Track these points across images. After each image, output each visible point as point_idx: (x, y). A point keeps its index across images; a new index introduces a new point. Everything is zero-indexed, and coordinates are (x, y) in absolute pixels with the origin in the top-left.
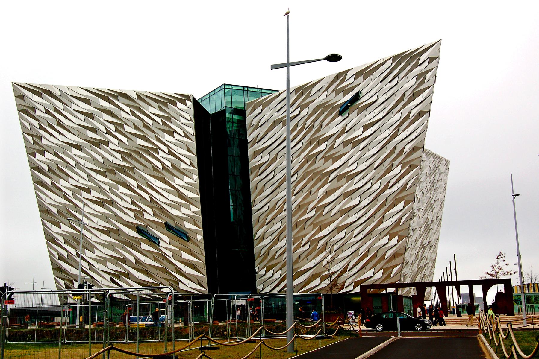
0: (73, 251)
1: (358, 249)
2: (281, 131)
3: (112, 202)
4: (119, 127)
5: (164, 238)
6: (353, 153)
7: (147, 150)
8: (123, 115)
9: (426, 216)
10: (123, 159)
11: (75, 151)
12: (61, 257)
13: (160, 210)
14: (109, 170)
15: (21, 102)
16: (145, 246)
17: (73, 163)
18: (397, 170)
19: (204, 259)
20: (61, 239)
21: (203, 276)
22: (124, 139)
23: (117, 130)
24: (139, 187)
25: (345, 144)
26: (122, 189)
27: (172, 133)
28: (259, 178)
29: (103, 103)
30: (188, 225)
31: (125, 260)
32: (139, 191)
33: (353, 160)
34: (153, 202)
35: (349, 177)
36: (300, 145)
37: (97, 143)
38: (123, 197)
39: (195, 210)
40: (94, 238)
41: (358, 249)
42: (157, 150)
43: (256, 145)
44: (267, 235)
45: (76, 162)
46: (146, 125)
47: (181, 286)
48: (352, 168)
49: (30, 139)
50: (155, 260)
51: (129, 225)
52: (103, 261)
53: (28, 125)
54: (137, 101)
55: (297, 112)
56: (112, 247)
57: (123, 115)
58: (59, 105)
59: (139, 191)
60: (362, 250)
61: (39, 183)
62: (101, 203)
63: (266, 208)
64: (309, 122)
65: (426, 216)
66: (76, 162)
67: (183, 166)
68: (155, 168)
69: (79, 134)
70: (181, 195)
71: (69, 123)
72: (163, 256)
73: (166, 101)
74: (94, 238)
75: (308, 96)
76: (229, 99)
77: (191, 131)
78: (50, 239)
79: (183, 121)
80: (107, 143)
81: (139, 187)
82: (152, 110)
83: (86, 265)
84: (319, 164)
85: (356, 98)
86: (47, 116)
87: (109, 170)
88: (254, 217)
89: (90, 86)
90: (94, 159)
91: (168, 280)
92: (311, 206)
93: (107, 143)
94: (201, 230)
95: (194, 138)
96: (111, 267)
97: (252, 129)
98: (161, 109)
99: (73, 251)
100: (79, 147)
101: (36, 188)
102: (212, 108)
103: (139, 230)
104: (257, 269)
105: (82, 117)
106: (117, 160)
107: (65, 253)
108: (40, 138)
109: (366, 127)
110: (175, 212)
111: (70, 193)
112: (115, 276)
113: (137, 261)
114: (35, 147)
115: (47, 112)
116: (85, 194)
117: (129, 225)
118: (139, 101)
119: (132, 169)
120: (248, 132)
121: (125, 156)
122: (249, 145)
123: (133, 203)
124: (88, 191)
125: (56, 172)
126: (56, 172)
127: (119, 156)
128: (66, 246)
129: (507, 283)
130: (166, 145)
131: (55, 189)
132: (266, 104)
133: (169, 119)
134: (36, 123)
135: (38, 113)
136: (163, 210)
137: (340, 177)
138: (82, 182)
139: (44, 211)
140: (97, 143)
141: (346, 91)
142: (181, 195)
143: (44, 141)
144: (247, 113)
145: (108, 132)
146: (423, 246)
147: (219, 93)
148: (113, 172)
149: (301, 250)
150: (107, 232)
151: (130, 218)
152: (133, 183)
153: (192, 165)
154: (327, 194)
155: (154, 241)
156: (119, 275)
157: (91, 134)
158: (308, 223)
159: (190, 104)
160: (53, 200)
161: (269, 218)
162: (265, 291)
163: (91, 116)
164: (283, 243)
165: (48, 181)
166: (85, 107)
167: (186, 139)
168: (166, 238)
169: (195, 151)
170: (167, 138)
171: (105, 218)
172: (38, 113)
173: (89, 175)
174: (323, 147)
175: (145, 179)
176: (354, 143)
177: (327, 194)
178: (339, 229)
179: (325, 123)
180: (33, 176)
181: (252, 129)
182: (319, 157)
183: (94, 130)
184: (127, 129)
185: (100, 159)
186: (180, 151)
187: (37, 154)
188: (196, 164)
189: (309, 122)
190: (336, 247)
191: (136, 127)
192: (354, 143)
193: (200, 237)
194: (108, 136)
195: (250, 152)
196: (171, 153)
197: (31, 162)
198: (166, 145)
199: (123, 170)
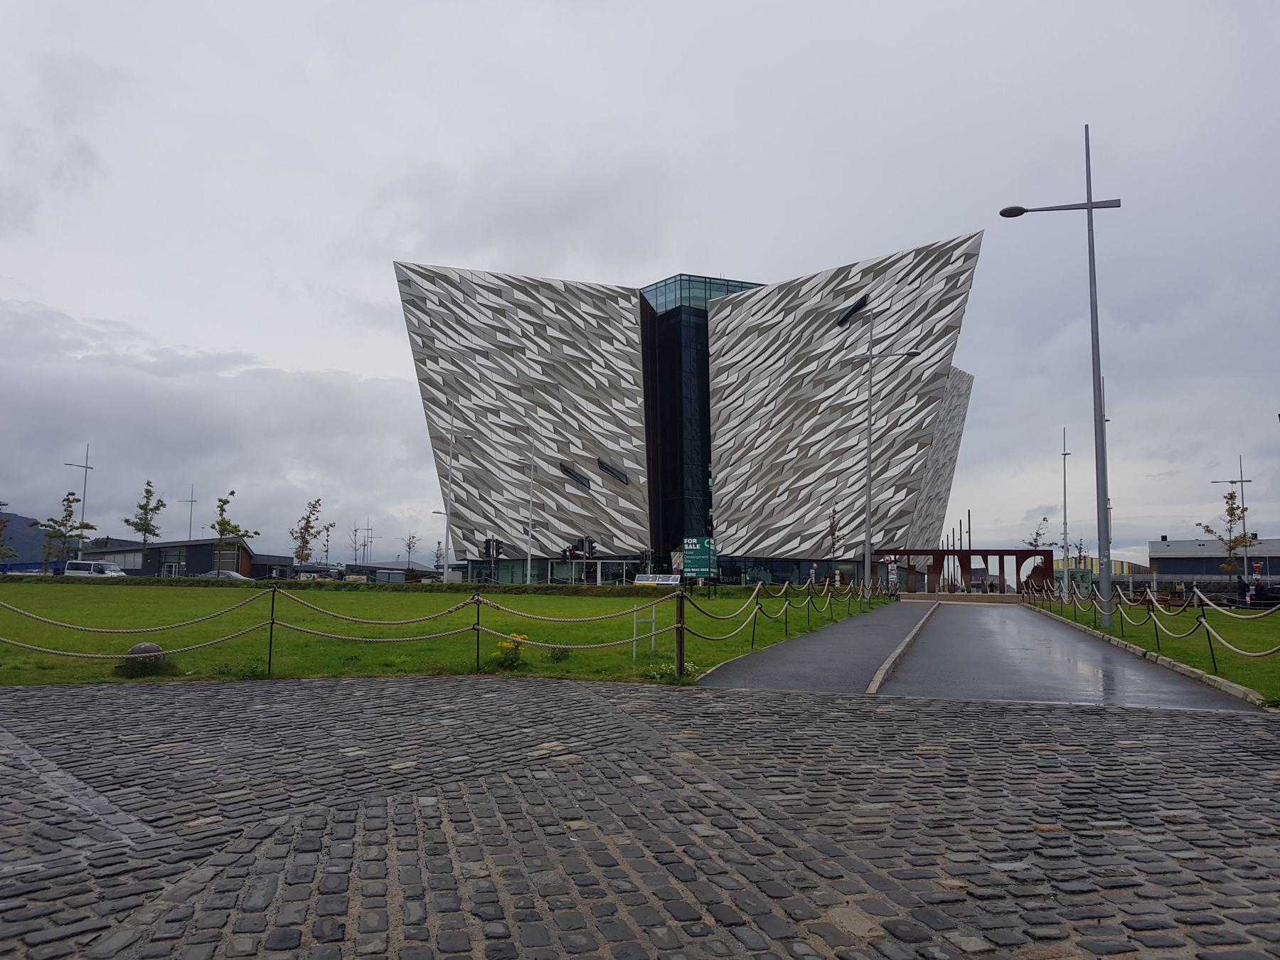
0: (475, 492)
1: (853, 503)
2: (756, 342)
3: (528, 430)
4: (540, 330)
5: (596, 478)
6: (851, 379)
8: (546, 312)
9: (935, 457)
10: (544, 373)
11: (480, 359)
12: (458, 499)
13: (591, 442)
14: (524, 387)
15: (406, 288)
16: (569, 489)
17: (477, 375)
19: (647, 507)
20: (459, 475)
21: (645, 531)
22: (546, 346)
23: (536, 334)
24: (565, 410)
25: (843, 364)
26: (541, 412)
27: (610, 339)
28: (722, 404)
29: (518, 295)
31: (543, 506)
32: (564, 416)
35: (846, 409)
36: (781, 363)
37: (511, 350)
39: (639, 443)
40: (503, 476)
41: (853, 503)
42: (590, 361)
43: (721, 360)
44: (729, 482)
45: (481, 374)
46: (575, 327)
47: (617, 542)
48: (851, 397)
49: (419, 340)
50: (583, 507)
51: (550, 460)
52: (515, 506)
53: (415, 321)
54: (567, 295)
55: (780, 317)
56: (524, 487)
57: (546, 312)
58: (459, 295)
59: (564, 416)
60: (857, 504)
61: (429, 400)
62: (514, 430)
63: (731, 444)
64: (795, 332)
65: (935, 457)
66: (481, 374)
67: (624, 384)
68: (586, 386)
71: (471, 321)
72: (594, 502)
73: (603, 297)
74: (503, 476)
75: (796, 297)
76: (686, 293)
77: (636, 338)
78: (444, 474)
79: (626, 323)
80: (522, 350)
81: (565, 410)
82: (585, 307)
83: (491, 510)
84: (806, 390)
86: (441, 309)
87: (524, 387)
88: (714, 455)
89: (502, 271)
90: (505, 370)
91: (599, 534)
92: (792, 445)
95: (640, 348)
97: (715, 337)
98: (596, 307)
99: (475, 492)
100: (485, 354)
101: (426, 407)
102: (661, 304)
103: (564, 468)
104: (715, 523)
105: (489, 313)
106: (536, 373)
107: (463, 494)
108: (432, 339)
110: (611, 445)
111: (472, 415)
113: (559, 506)
114: (424, 352)
115: (441, 304)
116: (491, 417)
117: (550, 460)
118: (566, 295)
119: (556, 387)
120: (711, 341)
121: (547, 369)
122: (711, 359)
123: (556, 431)
124: (496, 413)
125: (455, 386)
126: (455, 386)
127: (538, 368)
128: (464, 485)
129: (1048, 555)
130: (603, 356)
131: (451, 409)
132: (737, 305)
133: (607, 321)
134: (426, 319)
135: (430, 305)
137: (832, 409)
138: (487, 401)
139: (438, 439)
140: (511, 350)
143: (438, 344)
144: (710, 315)
145: (525, 335)
146: (929, 499)
147: (672, 286)
148: (531, 390)
149: (776, 500)
150: (521, 468)
151: (552, 452)
152: (557, 405)
153: (636, 384)
154: (814, 430)
155: (583, 482)
156: (536, 524)
157: (501, 337)
158: (787, 467)
159: (635, 300)
160: (446, 422)
161: (735, 457)
162: (724, 553)
163: (500, 312)
164: (751, 491)
165: (442, 398)
167: (628, 349)
168: (598, 480)
169: (640, 365)
171: (516, 448)
172: (430, 305)
173: (497, 392)
175: (573, 401)
177: (814, 430)
178: (828, 477)
179: (817, 335)
180: (423, 389)
181: (715, 337)
182: (807, 380)
183: (507, 332)
184: (551, 332)
186: (620, 364)
188: (641, 383)
189: (795, 332)
190: (824, 498)
191: (562, 331)
193: (643, 480)
194: (524, 340)
195: (713, 368)
196: (608, 367)
197: (419, 370)
198: (603, 356)
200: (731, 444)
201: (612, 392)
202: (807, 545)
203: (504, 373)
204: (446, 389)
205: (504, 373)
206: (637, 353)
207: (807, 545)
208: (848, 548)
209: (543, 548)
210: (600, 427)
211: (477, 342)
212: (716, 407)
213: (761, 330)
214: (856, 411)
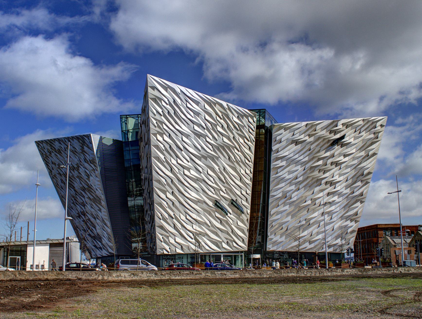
7: (228, 147)
18: (359, 184)
23: (213, 129)
25: (332, 164)
26: (210, 172)
29: (207, 107)
30: (244, 203)
33: (335, 174)
35: (332, 183)
48: (337, 178)
62: (196, 180)
79: (251, 131)
82: (236, 119)
85: (343, 137)
86: (168, 107)
90: (195, 147)
93: (205, 136)
94: (249, 206)
100: (187, 136)
109: (345, 156)
112: (196, 235)
116: (186, 172)
122: (272, 153)
124: (188, 169)
136: (231, 190)
140: (199, 135)
141: (335, 133)
143: (165, 127)
144: (273, 131)
148: (205, 158)
156: (200, 234)
157: (196, 128)
163: (197, 114)
165: (162, 157)
166: (197, 108)
167: (249, 143)
170: (241, 141)
174: (320, 162)
176: (337, 164)
184: (220, 129)
187: (158, 135)
192: (337, 164)
193: (249, 211)
200: (280, 195)
201: (241, 163)
202: (312, 245)
204: (165, 152)
207: (312, 245)
208: (329, 247)
212: (273, 176)
213: (297, 142)
214: (337, 185)
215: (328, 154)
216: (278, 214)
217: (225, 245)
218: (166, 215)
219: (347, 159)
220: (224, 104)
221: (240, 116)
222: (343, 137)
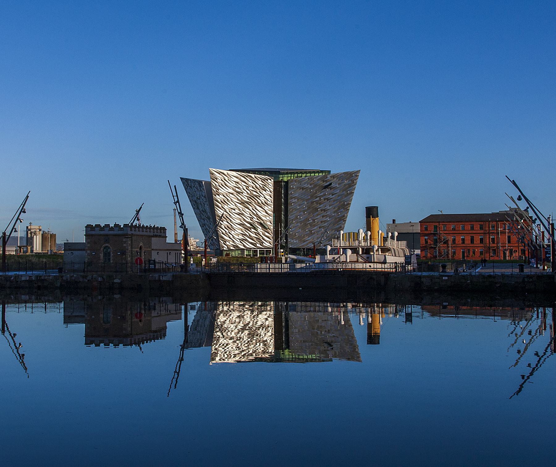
3: (243, 214)
4: (247, 188)
14: (242, 203)
16: (253, 230)
26: (247, 210)
31: (245, 235)
34: (257, 215)
38: (247, 213)
47: (264, 244)
69: (233, 189)
70: (266, 213)
77: (272, 190)
85: (331, 184)
87: (242, 203)
96: (241, 237)
100: (232, 194)
103: (251, 225)
107: (224, 232)
116: (233, 211)
124: (234, 210)
138: (232, 207)
141: (326, 181)
142: (266, 213)
159: (272, 180)
168: (260, 227)
174: (318, 199)
176: (328, 199)
183: (239, 188)
185: (240, 198)
186: (268, 197)
191: (253, 188)
193: (272, 228)
199: (247, 203)
203: (238, 199)
205: (238, 199)
206: (272, 195)
209: (244, 246)
210: (262, 214)
211: (231, 191)
213: (303, 189)
215: (322, 194)
216: (294, 228)
217: (258, 245)
218: (224, 232)
219: (334, 196)
220: (253, 175)
221: (263, 180)
222: (331, 184)
